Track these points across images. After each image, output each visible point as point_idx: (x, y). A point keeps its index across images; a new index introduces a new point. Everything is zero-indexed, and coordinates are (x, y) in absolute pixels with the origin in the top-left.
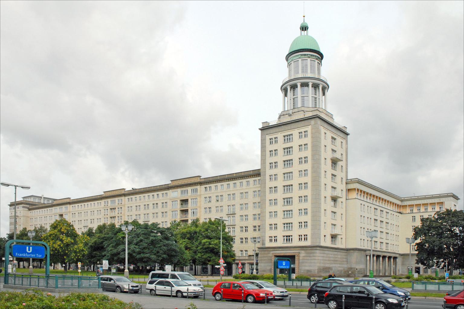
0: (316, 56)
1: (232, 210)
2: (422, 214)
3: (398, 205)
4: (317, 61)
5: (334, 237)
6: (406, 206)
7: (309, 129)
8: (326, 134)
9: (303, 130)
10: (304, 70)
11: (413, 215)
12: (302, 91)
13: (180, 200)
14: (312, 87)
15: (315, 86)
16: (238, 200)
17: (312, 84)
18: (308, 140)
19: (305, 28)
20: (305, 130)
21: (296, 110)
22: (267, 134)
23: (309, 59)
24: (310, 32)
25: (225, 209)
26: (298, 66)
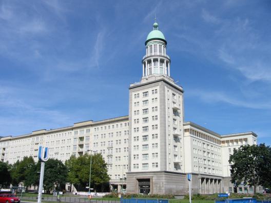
1: (111, 144)
2: (235, 147)
7: (158, 88)
9: (154, 89)
11: (229, 148)
18: (158, 95)
20: (156, 88)
23: (158, 44)
25: (107, 143)
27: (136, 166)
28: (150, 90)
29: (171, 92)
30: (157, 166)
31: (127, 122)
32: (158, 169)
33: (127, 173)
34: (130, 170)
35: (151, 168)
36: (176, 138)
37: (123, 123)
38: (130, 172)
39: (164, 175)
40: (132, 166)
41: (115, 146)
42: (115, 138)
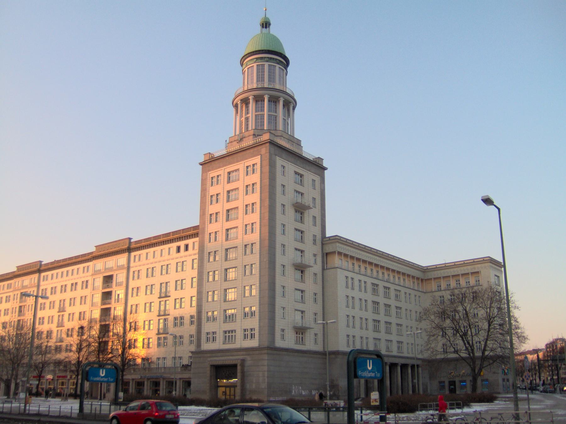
0: (276, 59)
3: (418, 279)
4: (278, 66)
5: (300, 331)
6: (431, 279)
7: (257, 160)
8: (287, 170)
10: (260, 78)
15: (274, 100)
16: (172, 277)
17: (269, 98)
18: (256, 178)
19: (266, 24)
23: (267, 64)
24: (273, 30)
26: (252, 74)
27: (212, 337)
28: (241, 166)
29: (291, 168)
30: (252, 336)
31: (197, 239)
32: (254, 343)
33: (192, 352)
34: (199, 344)
35: (240, 343)
36: (301, 268)
39: (266, 357)
41: (174, 294)
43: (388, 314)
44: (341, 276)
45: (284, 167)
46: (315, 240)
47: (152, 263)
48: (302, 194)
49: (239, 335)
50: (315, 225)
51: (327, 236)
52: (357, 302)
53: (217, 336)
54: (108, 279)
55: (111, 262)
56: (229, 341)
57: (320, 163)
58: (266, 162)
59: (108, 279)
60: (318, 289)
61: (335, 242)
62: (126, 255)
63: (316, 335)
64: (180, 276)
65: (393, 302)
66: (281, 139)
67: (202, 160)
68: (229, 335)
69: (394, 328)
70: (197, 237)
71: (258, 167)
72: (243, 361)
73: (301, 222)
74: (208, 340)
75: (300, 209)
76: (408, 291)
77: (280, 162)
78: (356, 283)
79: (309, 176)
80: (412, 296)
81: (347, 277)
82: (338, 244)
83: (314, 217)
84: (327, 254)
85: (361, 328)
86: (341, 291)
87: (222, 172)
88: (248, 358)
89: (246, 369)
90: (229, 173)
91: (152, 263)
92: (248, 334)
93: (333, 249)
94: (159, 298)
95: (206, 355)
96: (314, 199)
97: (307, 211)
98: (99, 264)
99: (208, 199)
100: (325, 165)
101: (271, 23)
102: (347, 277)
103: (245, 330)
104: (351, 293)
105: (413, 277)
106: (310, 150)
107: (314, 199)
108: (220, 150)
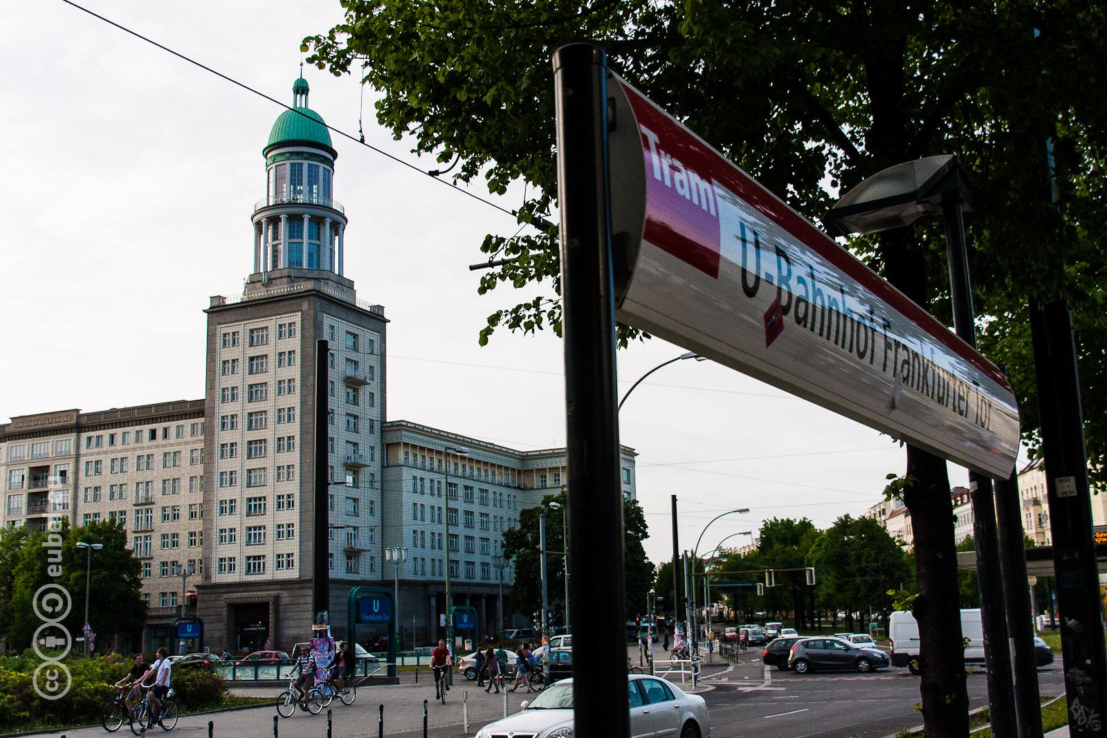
3: (513, 470)
4: (322, 166)
6: (532, 471)
7: (297, 318)
8: (337, 330)
12: (290, 227)
13: (30, 468)
14: (310, 220)
15: (317, 221)
18: (295, 343)
21: (277, 274)
22: (219, 324)
23: (306, 163)
25: (130, 491)
27: (228, 564)
28: (272, 323)
29: (342, 326)
32: (293, 574)
33: (197, 587)
34: (208, 577)
35: (271, 573)
37: (187, 423)
38: (207, 583)
40: (215, 565)
42: (158, 473)
43: (469, 525)
44: (407, 475)
45: (332, 327)
46: (372, 427)
47: (120, 451)
48: (356, 363)
49: (270, 562)
50: (372, 405)
51: (388, 421)
52: (428, 510)
53: (237, 563)
54: (39, 474)
55: (45, 448)
56: (254, 571)
57: (380, 313)
58: (309, 324)
59: (39, 474)
60: (376, 495)
61: (400, 430)
62: (73, 436)
63: (372, 558)
64: (171, 473)
65: (476, 508)
66: (327, 284)
67: (207, 306)
68: (255, 563)
69: (477, 544)
70: (202, 417)
71: (298, 327)
72: (277, 598)
73: (354, 404)
74: (221, 569)
75: (354, 384)
76: (498, 489)
77: (327, 321)
78: (427, 484)
79: (366, 335)
80: (505, 497)
81: (415, 478)
82: (404, 432)
83: (372, 395)
84: (388, 445)
85: (433, 547)
86: (408, 498)
87: (242, 328)
88: (284, 594)
89: (281, 609)
90: (252, 331)
91: (120, 451)
92: (283, 561)
93: (394, 437)
94: (135, 505)
95: (219, 591)
96: (372, 368)
97: (362, 387)
98: (23, 448)
99: (219, 366)
100: (387, 316)
101: (310, 88)
102: (415, 478)
103: (279, 556)
104: (419, 499)
105: (507, 468)
106: (364, 299)
107: (372, 368)
108: (235, 294)
